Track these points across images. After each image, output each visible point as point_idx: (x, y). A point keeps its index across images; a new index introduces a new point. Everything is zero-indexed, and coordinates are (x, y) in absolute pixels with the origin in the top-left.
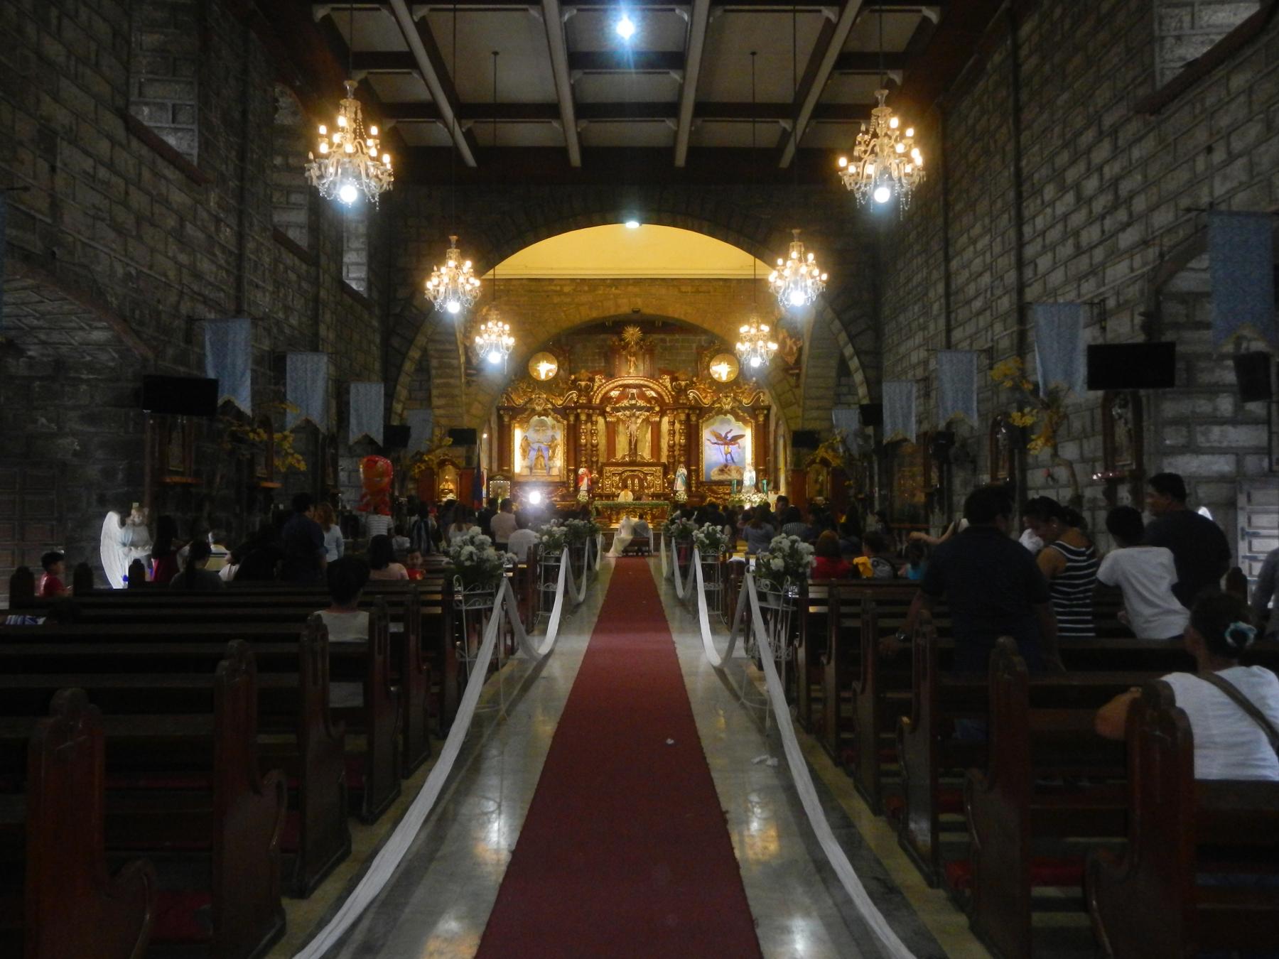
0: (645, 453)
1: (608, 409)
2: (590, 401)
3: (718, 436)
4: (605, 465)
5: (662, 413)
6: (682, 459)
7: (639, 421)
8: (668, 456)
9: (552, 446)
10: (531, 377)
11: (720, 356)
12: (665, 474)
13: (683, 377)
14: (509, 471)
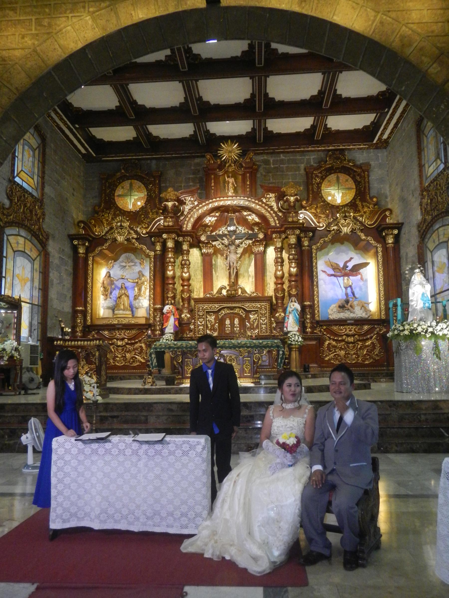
0: (247, 285)
1: (203, 238)
2: (181, 227)
3: (335, 267)
4: (198, 301)
5: (267, 241)
6: (294, 292)
7: (240, 250)
8: (276, 290)
9: (139, 285)
10: (117, 208)
11: (333, 177)
12: (273, 310)
13: (293, 191)
14: (84, 313)
